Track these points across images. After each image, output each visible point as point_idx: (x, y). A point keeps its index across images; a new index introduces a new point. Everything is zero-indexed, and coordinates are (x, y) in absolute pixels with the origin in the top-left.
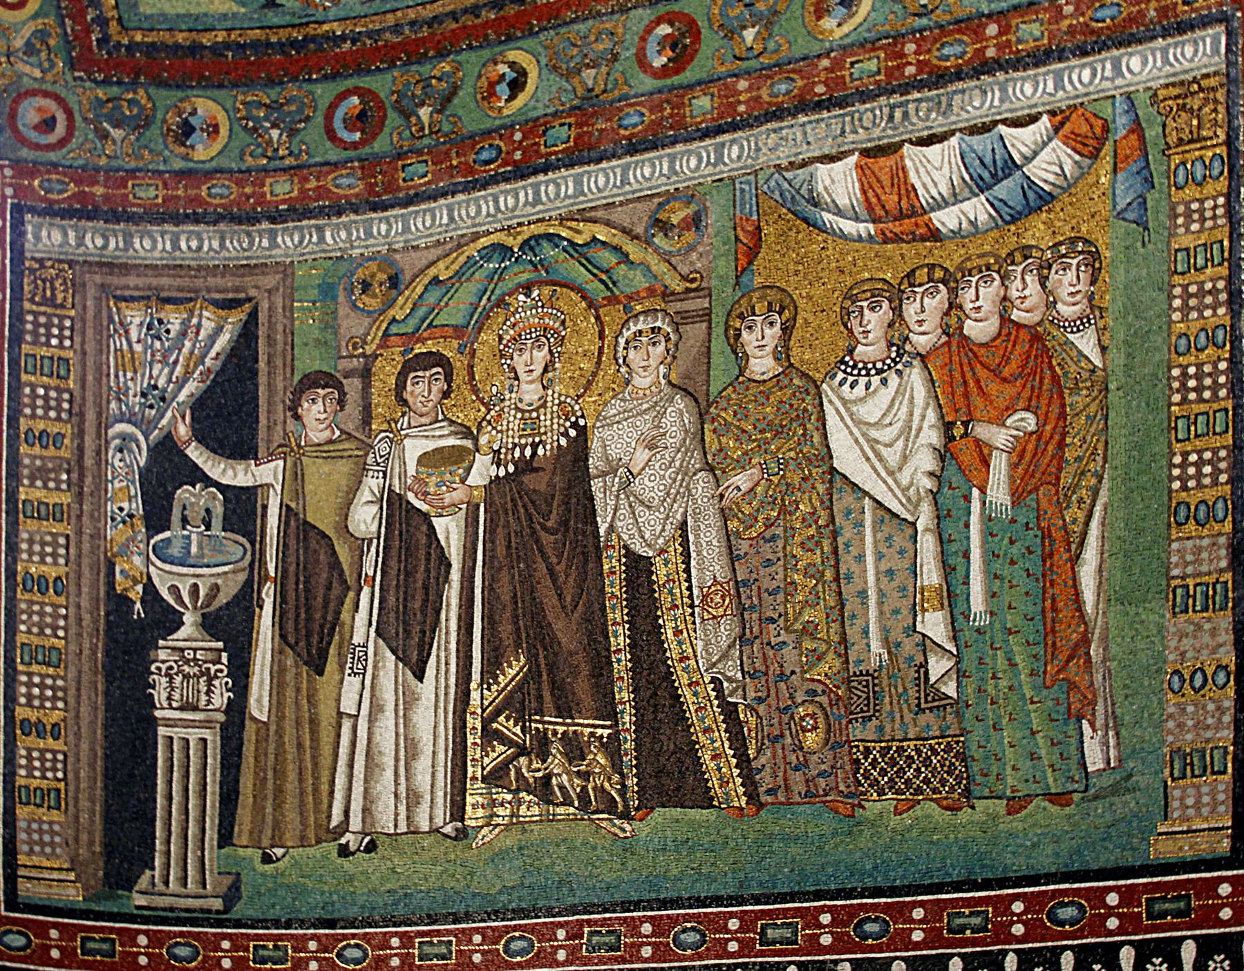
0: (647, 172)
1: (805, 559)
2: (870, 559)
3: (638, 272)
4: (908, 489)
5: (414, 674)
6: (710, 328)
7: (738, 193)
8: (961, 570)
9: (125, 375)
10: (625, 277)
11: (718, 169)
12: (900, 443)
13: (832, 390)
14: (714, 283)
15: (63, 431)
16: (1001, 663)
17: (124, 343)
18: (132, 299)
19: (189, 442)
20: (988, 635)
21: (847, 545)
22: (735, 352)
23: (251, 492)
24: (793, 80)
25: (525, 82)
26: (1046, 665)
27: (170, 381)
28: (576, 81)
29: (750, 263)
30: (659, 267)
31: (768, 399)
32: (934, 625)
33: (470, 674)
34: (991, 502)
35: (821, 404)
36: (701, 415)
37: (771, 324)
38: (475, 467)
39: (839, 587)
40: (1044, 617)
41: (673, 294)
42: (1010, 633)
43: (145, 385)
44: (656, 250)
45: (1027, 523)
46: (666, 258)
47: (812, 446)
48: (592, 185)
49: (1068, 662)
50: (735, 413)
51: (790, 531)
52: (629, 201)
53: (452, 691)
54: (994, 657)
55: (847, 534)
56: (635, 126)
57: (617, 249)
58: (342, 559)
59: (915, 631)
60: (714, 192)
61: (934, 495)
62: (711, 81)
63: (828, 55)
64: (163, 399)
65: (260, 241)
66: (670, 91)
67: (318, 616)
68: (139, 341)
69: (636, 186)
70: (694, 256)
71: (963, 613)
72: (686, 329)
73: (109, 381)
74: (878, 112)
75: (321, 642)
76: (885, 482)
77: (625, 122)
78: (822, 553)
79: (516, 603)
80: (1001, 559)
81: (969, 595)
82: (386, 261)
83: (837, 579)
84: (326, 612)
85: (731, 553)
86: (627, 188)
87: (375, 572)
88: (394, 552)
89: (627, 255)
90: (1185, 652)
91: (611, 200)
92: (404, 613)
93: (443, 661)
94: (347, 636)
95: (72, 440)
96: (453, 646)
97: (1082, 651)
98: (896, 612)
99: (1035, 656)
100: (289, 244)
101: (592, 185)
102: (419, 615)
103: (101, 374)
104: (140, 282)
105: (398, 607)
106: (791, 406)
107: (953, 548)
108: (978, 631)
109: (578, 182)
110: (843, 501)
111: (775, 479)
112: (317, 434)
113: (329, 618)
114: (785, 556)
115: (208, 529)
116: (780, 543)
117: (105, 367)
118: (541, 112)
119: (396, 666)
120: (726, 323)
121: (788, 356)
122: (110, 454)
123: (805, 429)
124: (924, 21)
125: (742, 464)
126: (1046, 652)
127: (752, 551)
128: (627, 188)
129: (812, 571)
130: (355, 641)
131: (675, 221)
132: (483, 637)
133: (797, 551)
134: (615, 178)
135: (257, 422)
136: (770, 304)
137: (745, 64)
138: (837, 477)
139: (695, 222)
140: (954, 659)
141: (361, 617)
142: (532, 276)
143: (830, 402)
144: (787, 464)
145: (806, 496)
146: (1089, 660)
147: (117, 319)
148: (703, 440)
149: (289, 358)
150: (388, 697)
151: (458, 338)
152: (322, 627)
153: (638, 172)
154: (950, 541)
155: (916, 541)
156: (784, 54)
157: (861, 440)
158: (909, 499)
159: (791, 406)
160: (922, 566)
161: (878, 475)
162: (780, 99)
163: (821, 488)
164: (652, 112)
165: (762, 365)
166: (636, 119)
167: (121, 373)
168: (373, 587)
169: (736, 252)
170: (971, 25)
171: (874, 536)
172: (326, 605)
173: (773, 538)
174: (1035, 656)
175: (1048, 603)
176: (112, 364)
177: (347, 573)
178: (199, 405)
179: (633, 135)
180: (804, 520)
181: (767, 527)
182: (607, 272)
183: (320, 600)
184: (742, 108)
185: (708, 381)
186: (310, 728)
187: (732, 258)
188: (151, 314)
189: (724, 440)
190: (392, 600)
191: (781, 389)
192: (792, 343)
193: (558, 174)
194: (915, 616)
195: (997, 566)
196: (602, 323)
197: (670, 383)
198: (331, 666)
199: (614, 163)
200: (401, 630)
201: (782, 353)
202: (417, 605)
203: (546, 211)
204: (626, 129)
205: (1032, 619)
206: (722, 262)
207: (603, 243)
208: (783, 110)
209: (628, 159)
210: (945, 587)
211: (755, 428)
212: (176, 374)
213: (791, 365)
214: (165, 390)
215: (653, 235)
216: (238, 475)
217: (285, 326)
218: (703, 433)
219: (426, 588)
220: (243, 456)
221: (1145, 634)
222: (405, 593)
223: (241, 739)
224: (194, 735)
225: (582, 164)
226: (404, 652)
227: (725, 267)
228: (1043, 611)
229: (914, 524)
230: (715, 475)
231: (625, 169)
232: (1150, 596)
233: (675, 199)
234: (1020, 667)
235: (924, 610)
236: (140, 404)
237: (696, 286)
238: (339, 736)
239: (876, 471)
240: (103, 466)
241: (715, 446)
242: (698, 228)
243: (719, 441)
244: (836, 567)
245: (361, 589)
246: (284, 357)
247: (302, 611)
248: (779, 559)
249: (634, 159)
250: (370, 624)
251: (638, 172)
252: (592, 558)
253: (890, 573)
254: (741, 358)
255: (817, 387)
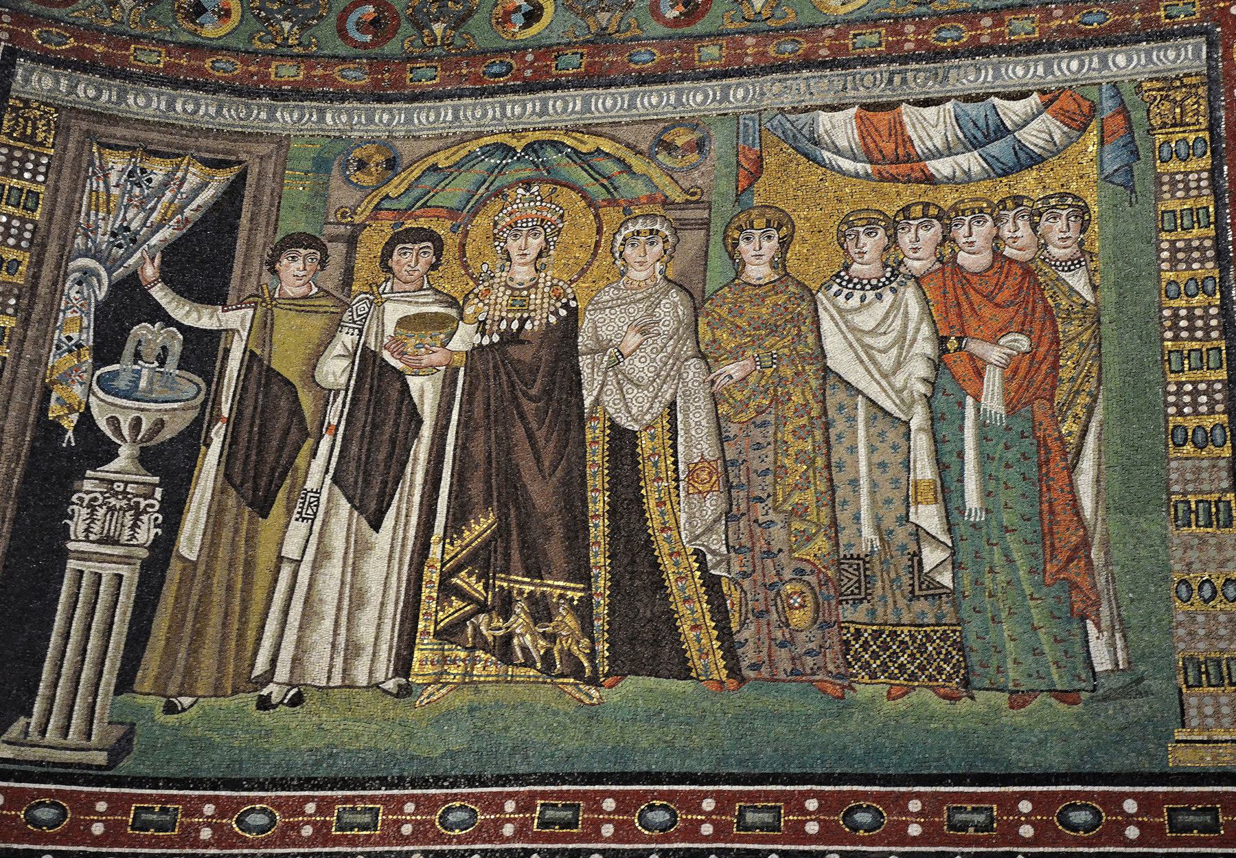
0: (654, 100)
1: (796, 446)
2: (862, 451)
3: (640, 182)
4: (902, 391)
5: (370, 522)
6: (708, 235)
7: (741, 127)
8: (954, 468)
9: (97, 215)
10: (627, 184)
11: (723, 106)
12: (894, 351)
13: (828, 299)
14: (714, 198)
15: (20, 259)
16: (998, 557)
17: (102, 185)
18: (117, 147)
19: (155, 283)
20: (984, 531)
21: (839, 437)
22: (732, 258)
23: (213, 336)
24: (800, 43)
25: (541, 15)
26: (1045, 562)
27: (144, 225)
28: (590, 21)
29: (751, 185)
30: (661, 180)
31: (763, 301)
32: (928, 517)
33: (433, 527)
34: (985, 410)
35: (816, 310)
36: (695, 309)
37: (769, 237)
38: (458, 333)
39: (831, 474)
40: (1041, 519)
41: (673, 203)
42: (1007, 531)
43: (117, 226)
44: (659, 165)
45: (1023, 432)
46: (669, 173)
47: (806, 345)
48: (600, 106)
49: (1070, 560)
50: (730, 311)
51: (781, 421)
52: (637, 123)
53: (410, 543)
54: (991, 552)
55: (840, 426)
56: (645, 62)
57: (620, 161)
58: (304, 407)
59: (908, 521)
60: (719, 124)
61: (929, 400)
62: (719, 35)
63: (832, 27)
64: (134, 241)
65: (259, 114)
66: (680, 38)
67: (270, 458)
68: (117, 186)
69: (642, 111)
70: (696, 174)
71: (957, 508)
72: (687, 235)
73: (78, 217)
74: (878, 76)
75: (271, 482)
76: (879, 383)
77: (636, 58)
78: (814, 441)
79: (490, 463)
80: (995, 463)
81: (963, 491)
82: (384, 145)
83: (828, 466)
84: (280, 456)
85: (720, 434)
86: (634, 112)
87: (339, 422)
88: (362, 405)
89: (630, 167)
90: (1191, 563)
91: (617, 120)
92: (366, 463)
93: (404, 512)
94: (300, 481)
95: (28, 268)
96: (417, 499)
97: (1081, 553)
98: (888, 501)
99: (1033, 554)
100: (288, 119)
101: (600, 106)
102: (382, 467)
103: (71, 211)
104: (128, 133)
105: (360, 459)
106: (786, 309)
107: (947, 447)
108: (974, 525)
109: (586, 101)
110: (836, 397)
111: (768, 372)
112: (293, 288)
113: (283, 462)
114: (776, 441)
115: (161, 366)
116: (771, 430)
117: (77, 204)
118: (554, 41)
119: (351, 514)
120: (725, 232)
121: (784, 266)
122: (67, 285)
123: (800, 330)
124: (923, 9)
125: (735, 355)
126: (1044, 551)
127: (742, 434)
128: (634, 112)
129: (802, 457)
130: (308, 486)
131: (679, 142)
132: (450, 493)
133: (789, 438)
134: (623, 102)
135: (231, 272)
136: (768, 221)
137: (754, 25)
138: (831, 376)
139: (700, 146)
140: (949, 551)
141: (318, 464)
142: (534, 174)
143: (825, 309)
144: (779, 358)
145: (799, 389)
146: (1090, 562)
147: (97, 163)
148: (696, 332)
149: (274, 218)
150: (338, 542)
151: (451, 218)
152: (273, 470)
153: (646, 100)
154: (944, 442)
155: (909, 439)
156: (791, 19)
157: (855, 344)
158: (902, 401)
159: (786, 309)
160: (915, 462)
161: (872, 376)
162: (786, 55)
163: (814, 383)
164: (662, 53)
165: (758, 271)
166: (647, 57)
167: (93, 212)
168: (335, 435)
169: (737, 175)
170: (970, 16)
171: (867, 431)
172: (280, 449)
173: (764, 424)
174: (1033, 554)
175: (1045, 507)
176: (85, 203)
177: (308, 420)
178: (171, 251)
179: (643, 70)
180: (796, 410)
181: (759, 413)
182: (609, 178)
183: (275, 443)
184: (749, 59)
185: (704, 280)
186: (245, 571)
187: (733, 179)
188: (135, 163)
189: (718, 333)
190: (354, 449)
191: (777, 293)
192: (788, 255)
193: (566, 93)
194: (908, 506)
195: (992, 468)
196: (600, 220)
197: (665, 278)
198: (278, 509)
199: (623, 90)
200: (360, 480)
201: (781, 263)
202: (381, 457)
203: (552, 122)
204: (636, 63)
205: (1029, 520)
206: (723, 182)
207: (607, 154)
208: (788, 66)
209: (637, 88)
210: (939, 485)
211: (750, 325)
212: (151, 219)
213: (787, 274)
214: (137, 233)
215: (657, 153)
216: (204, 319)
217: (273, 191)
218: (697, 325)
219: (393, 441)
220: (212, 302)
221: (1148, 542)
222: (370, 443)
223: (163, 577)
224: (108, 570)
225: (590, 87)
226: (361, 501)
227: (726, 186)
228: (1041, 513)
229: (907, 423)
230: (707, 363)
231: (633, 97)
232: (1151, 508)
233: (680, 125)
234: (1018, 563)
235: (917, 503)
236: (109, 243)
237: (695, 199)
238: (276, 581)
239: (869, 372)
240: (57, 296)
241: (708, 337)
242: (701, 152)
243: (714, 335)
244: (828, 454)
245: (322, 436)
246: (269, 217)
247: (254, 452)
248: (769, 444)
249: (642, 88)
250: (327, 471)
251: (646, 100)
252: (575, 425)
253: (883, 465)
254: (739, 266)
255: (812, 295)
